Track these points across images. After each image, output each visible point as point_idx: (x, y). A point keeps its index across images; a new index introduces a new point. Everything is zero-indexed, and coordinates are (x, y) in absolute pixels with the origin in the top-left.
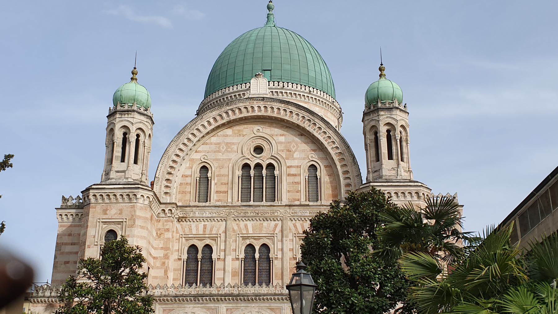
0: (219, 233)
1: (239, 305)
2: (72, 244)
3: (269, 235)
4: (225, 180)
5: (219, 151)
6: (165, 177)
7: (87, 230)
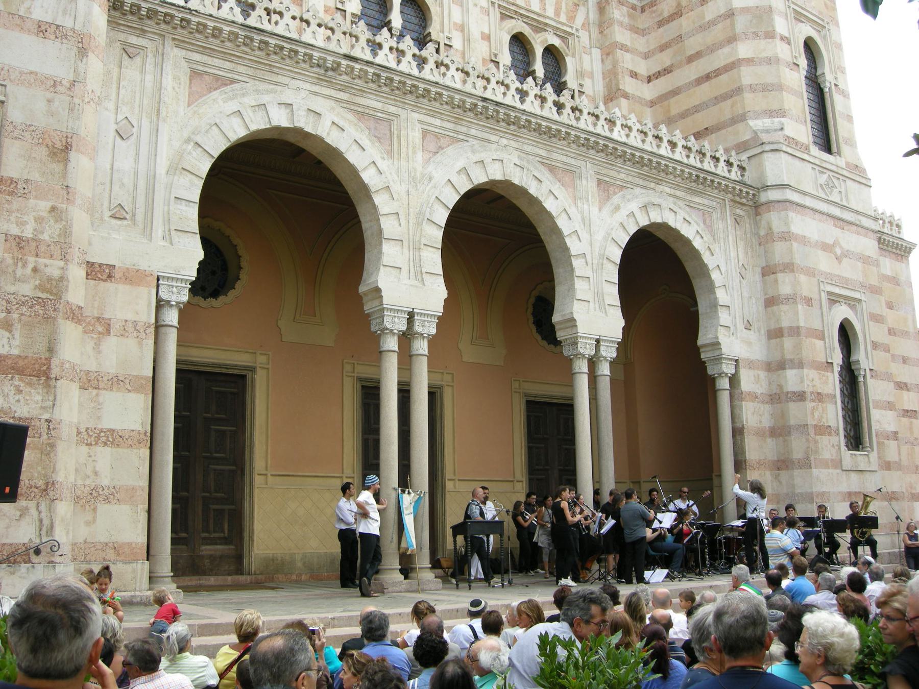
1: (464, 129)
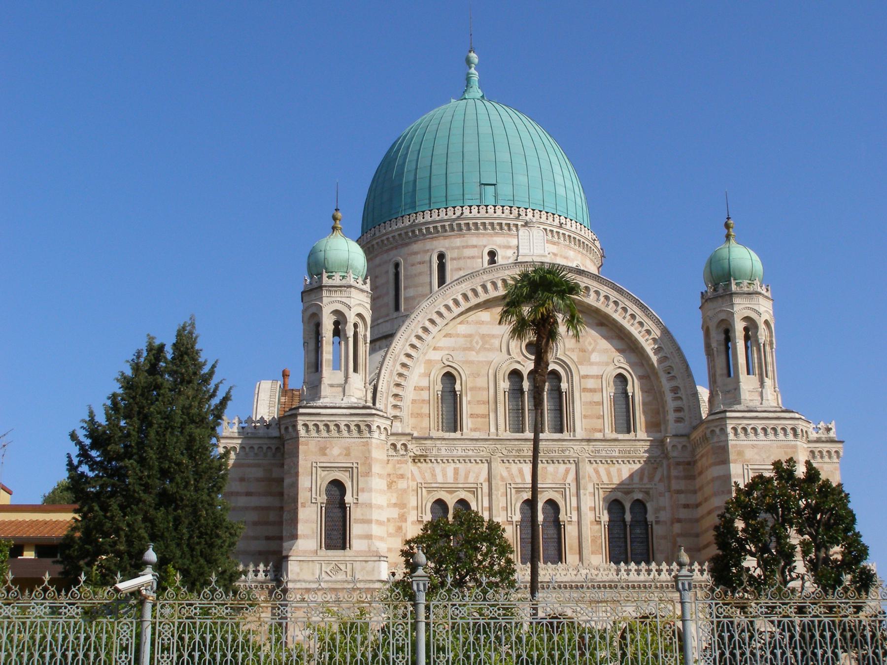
0: (479, 482)
2: (248, 494)
3: (558, 486)
4: (483, 396)
5: (470, 349)
6: (392, 392)
7: (297, 480)
